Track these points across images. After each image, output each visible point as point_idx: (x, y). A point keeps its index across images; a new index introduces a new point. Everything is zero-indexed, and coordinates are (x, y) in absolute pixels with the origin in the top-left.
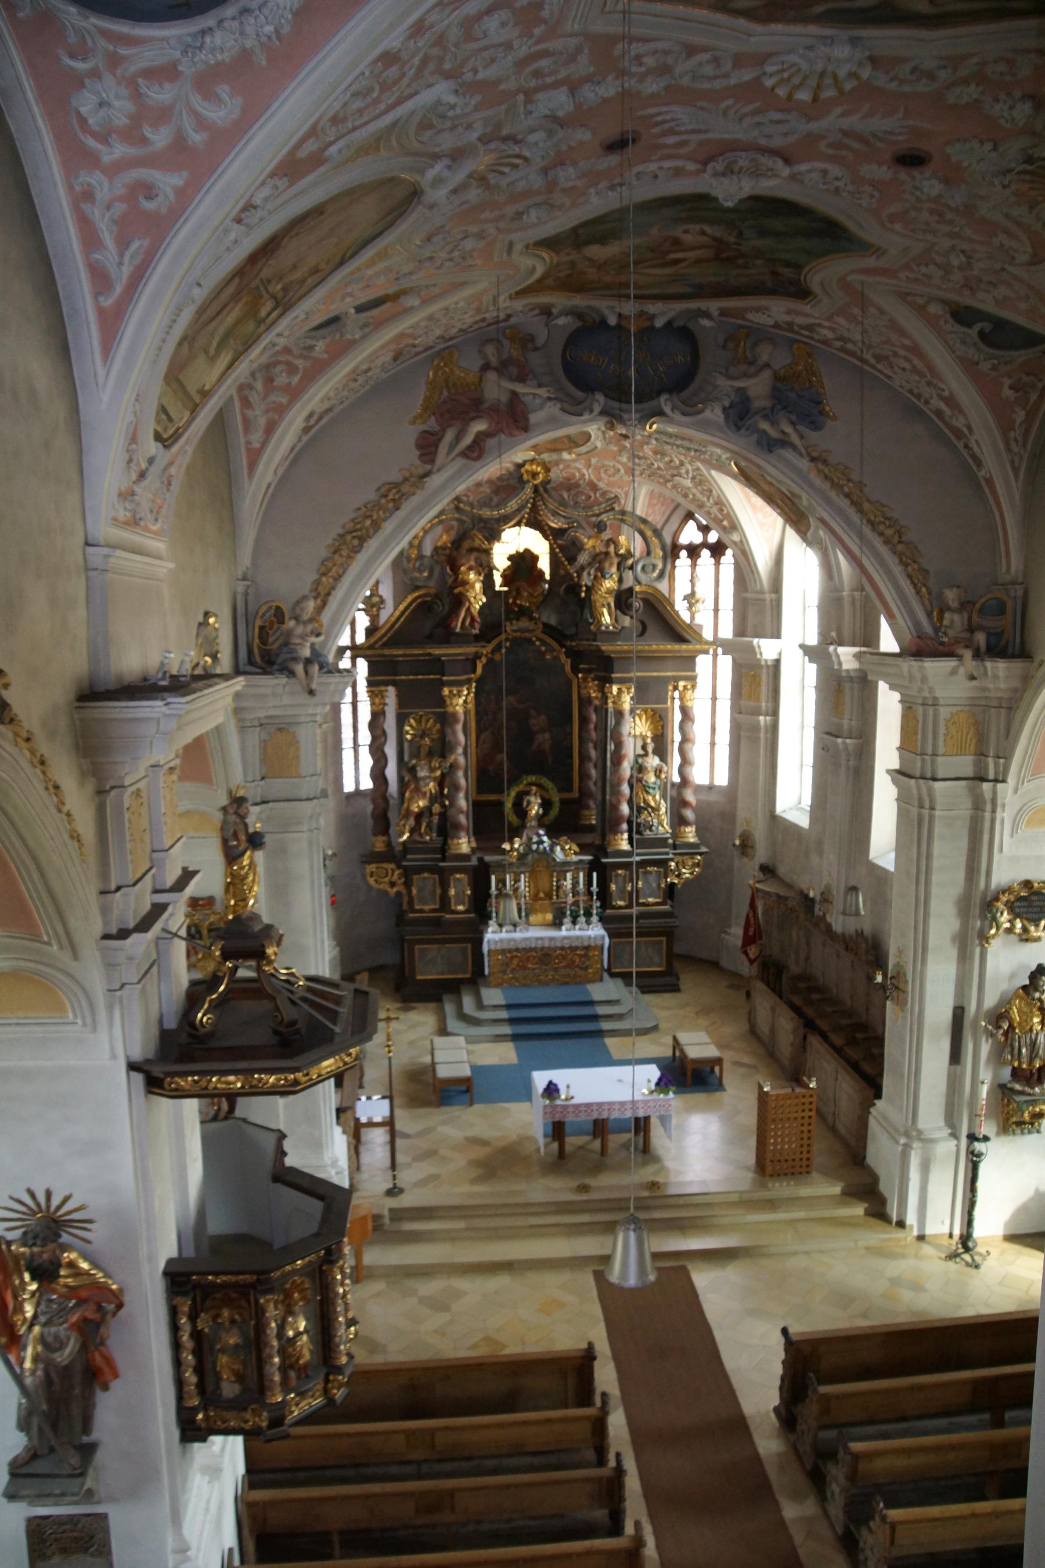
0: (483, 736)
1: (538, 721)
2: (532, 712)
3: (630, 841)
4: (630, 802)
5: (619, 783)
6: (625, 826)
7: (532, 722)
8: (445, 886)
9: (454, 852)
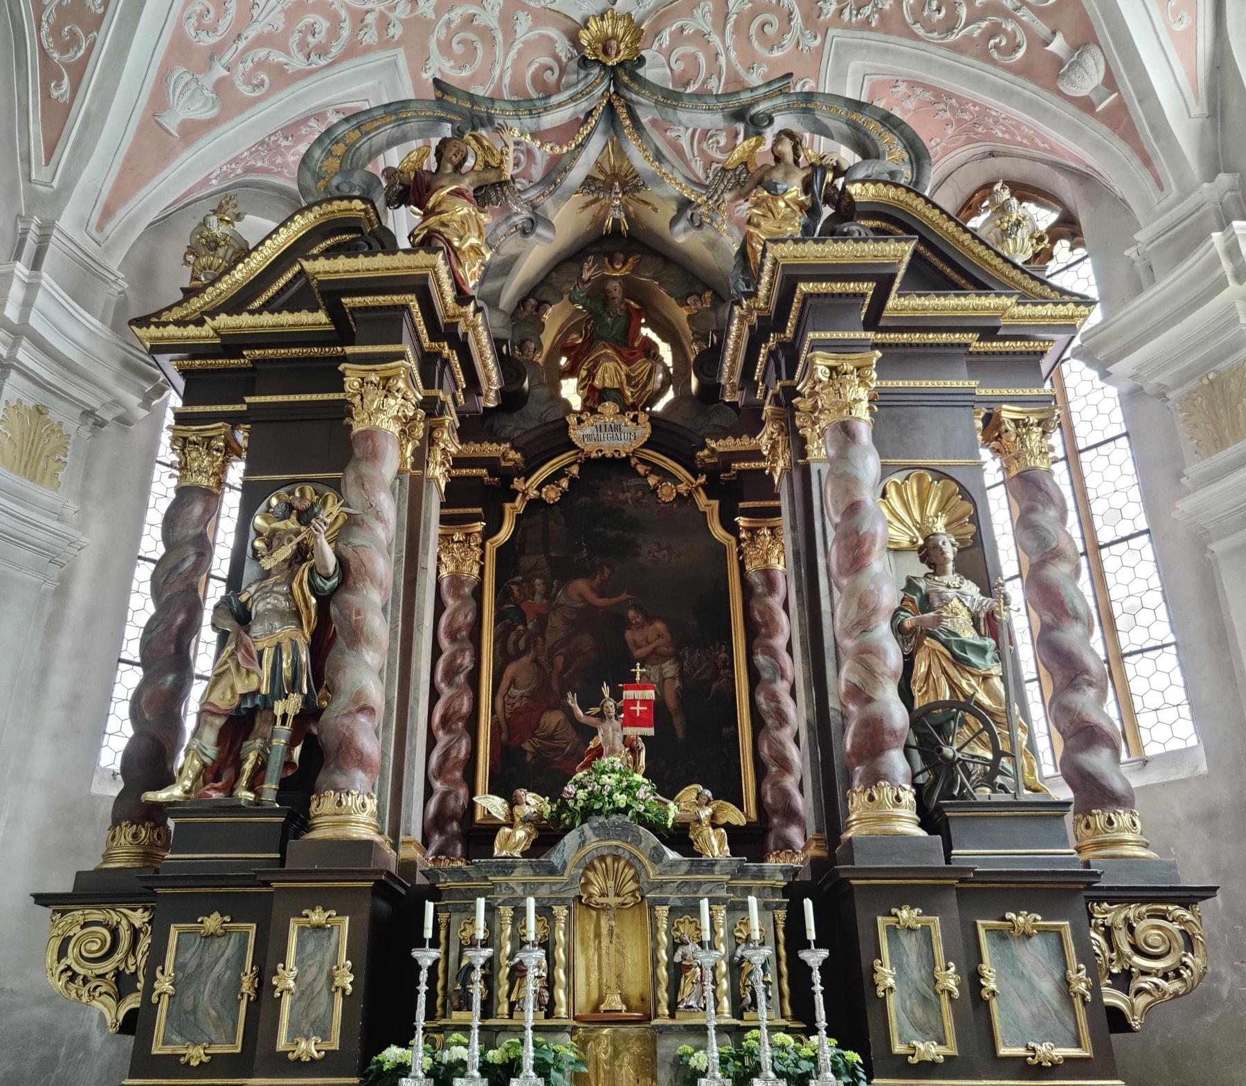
0: (511, 670)
1: (647, 635)
2: (631, 613)
3: (929, 818)
4: (906, 695)
5: (863, 625)
6: (896, 761)
7: (629, 635)
8: (268, 956)
9: (316, 835)
